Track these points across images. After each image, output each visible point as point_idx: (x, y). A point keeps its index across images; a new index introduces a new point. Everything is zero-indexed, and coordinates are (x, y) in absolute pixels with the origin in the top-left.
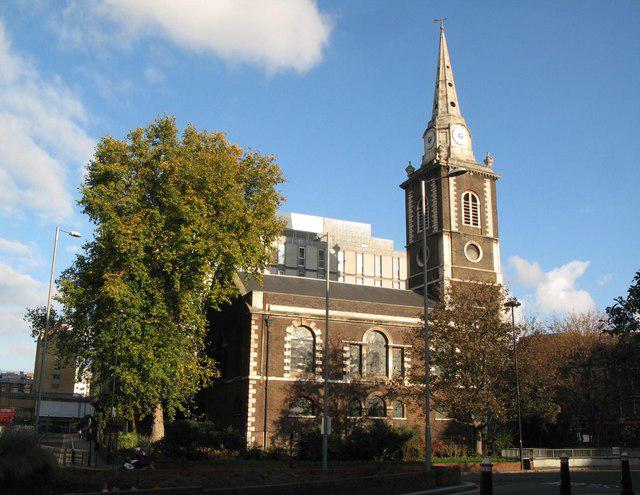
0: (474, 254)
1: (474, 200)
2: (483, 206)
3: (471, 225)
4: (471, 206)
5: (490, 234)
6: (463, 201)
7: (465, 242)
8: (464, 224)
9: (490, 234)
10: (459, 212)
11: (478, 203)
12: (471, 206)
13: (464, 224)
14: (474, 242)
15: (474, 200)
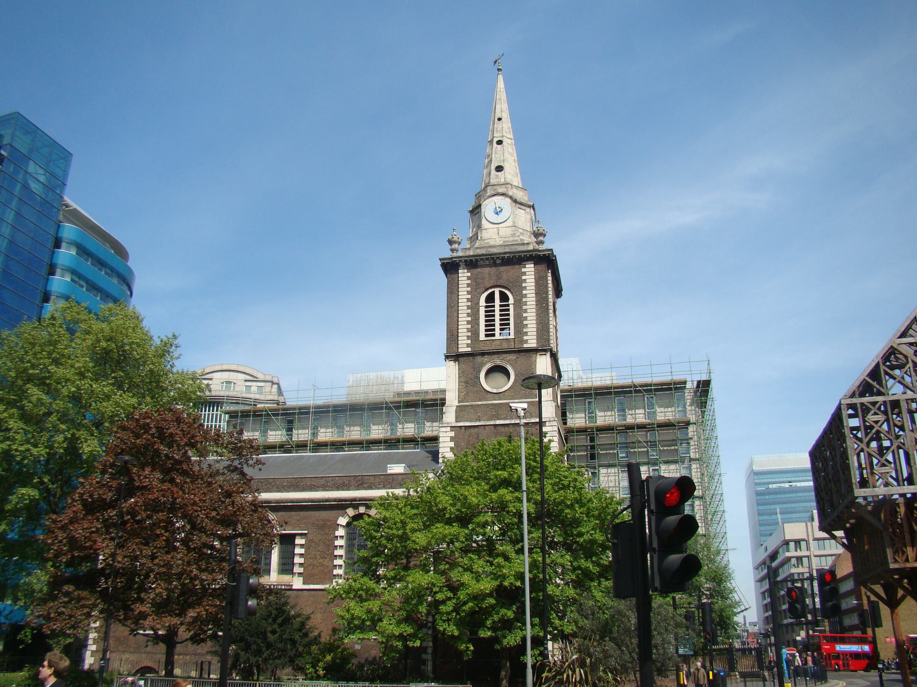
0: (499, 377)
1: (504, 297)
2: (519, 304)
3: (497, 337)
4: (497, 308)
5: (531, 342)
6: (482, 302)
7: (482, 365)
8: (482, 337)
9: (531, 342)
10: (474, 322)
11: (511, 301)
12: (497, 308)
13: (482, 337)
14: (499, 362)
15: (504, 297)
